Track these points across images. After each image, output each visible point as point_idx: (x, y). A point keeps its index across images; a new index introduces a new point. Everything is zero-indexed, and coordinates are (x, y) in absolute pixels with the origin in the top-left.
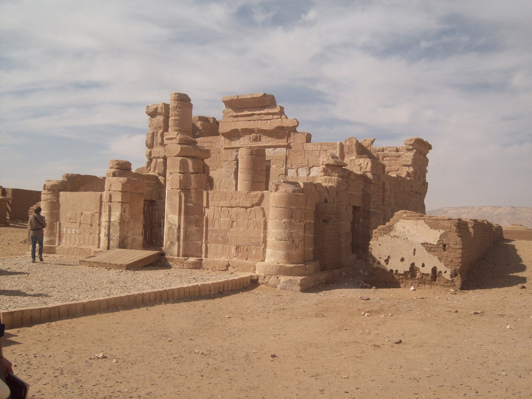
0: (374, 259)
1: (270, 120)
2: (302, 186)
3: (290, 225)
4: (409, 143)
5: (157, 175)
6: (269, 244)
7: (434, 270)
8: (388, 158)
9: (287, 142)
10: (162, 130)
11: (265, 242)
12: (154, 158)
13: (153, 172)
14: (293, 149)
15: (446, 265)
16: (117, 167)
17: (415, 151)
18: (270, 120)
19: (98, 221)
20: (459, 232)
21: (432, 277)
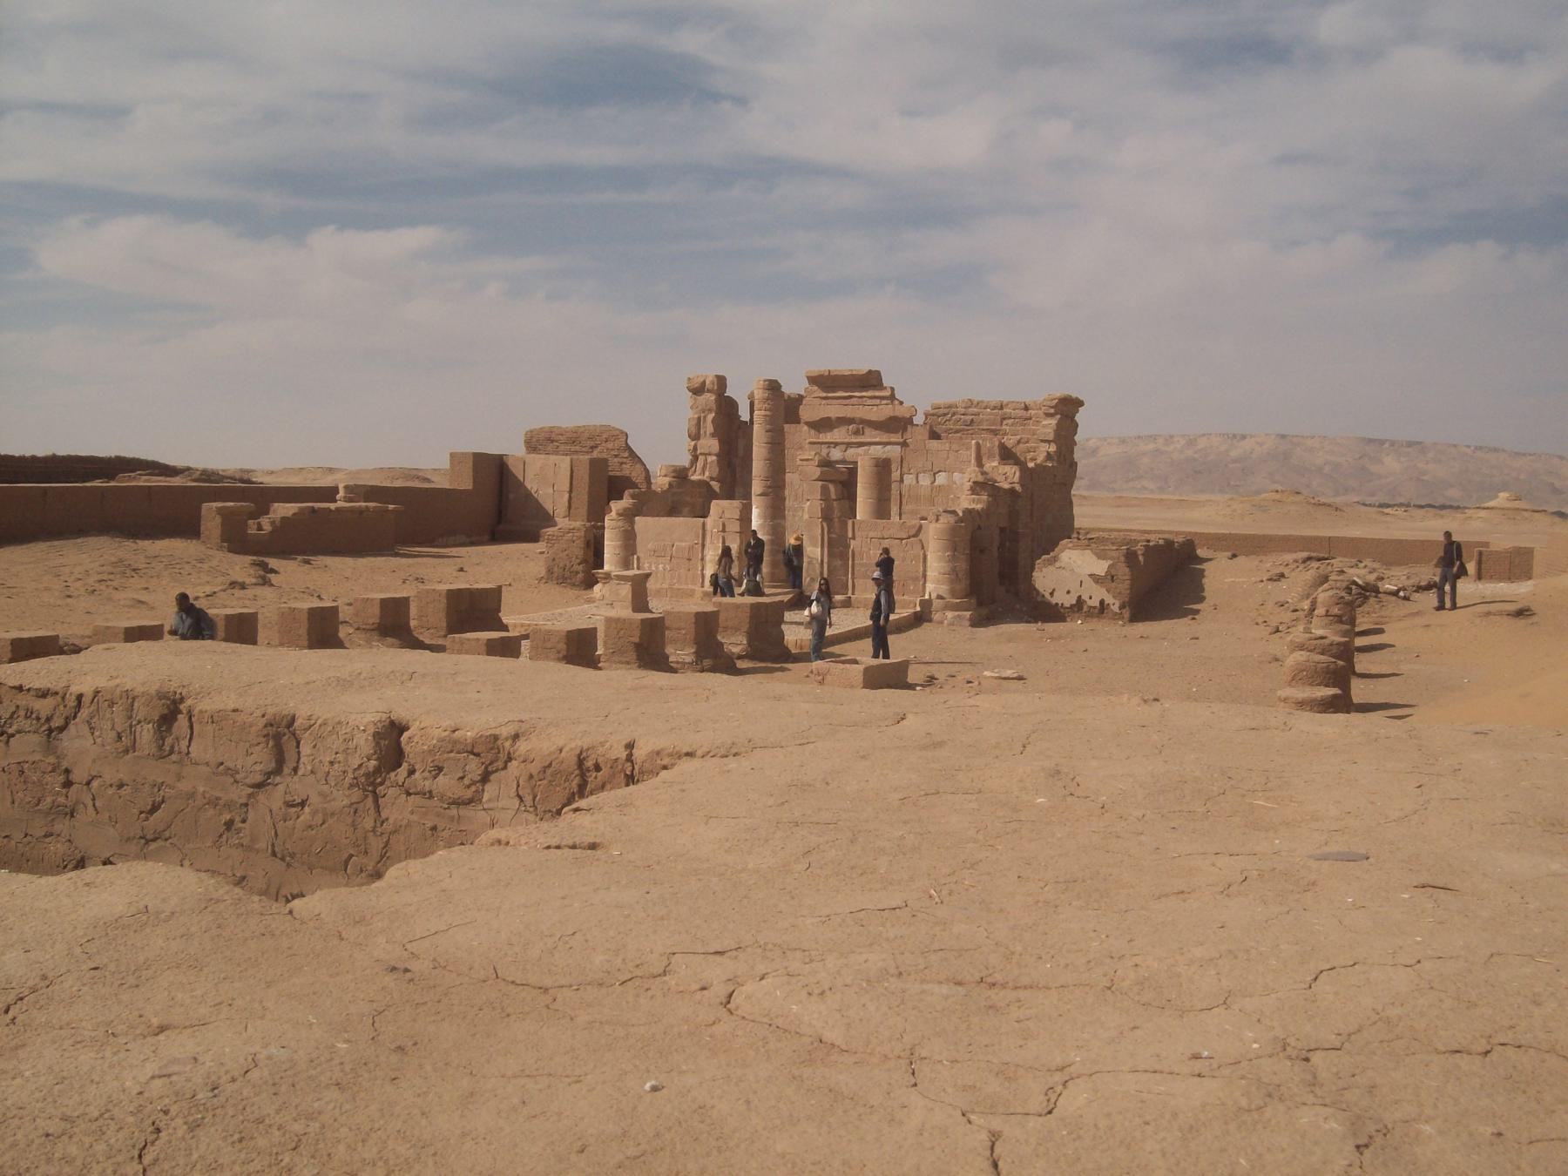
0: (1038, 591)
1: (877, 405)
2: (961, 514)
3: (953, 558)
4: (1049, 403)
5: (708, 480)
6: (928, 578)
7: (1102, 602)
8: (1010, 421)
9: (902, 438)
10: (714, 415)
11: (925, 576)
12: (701, 454)
13: (700, 474)
14: (911, 447)
15: (1114, 597)
16: (673, 474)
17: (1059, 416)
18: (877, 405)
19: (700, 555)
20: (1128, 563)
21: (1100, 610)
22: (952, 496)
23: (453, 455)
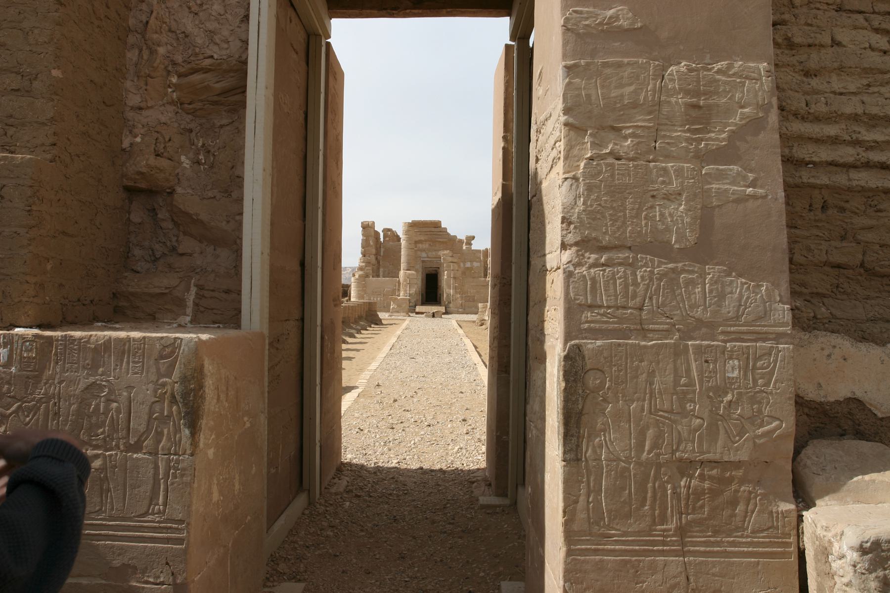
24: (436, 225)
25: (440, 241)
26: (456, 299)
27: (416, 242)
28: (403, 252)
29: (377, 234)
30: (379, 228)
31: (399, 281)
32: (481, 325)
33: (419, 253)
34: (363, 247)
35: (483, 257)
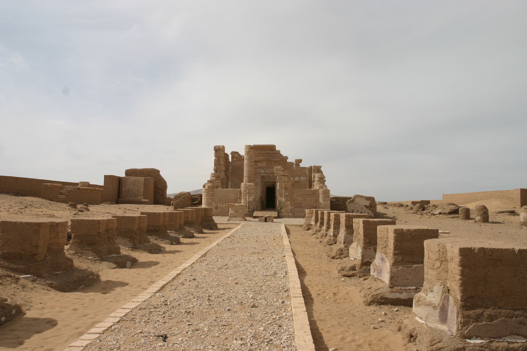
22: (300, 184)
23: (106, 177)
24: (272, 148)
25: (275, 161)
26: (287, 206)
27: (256, 162)
28: (245, 168)
29: (227, 155)
30: (228, 151)
31: (240, 191)
32: (308, 229)
33: (259, 170)
34: (215, 165)
35: (308, 173)
